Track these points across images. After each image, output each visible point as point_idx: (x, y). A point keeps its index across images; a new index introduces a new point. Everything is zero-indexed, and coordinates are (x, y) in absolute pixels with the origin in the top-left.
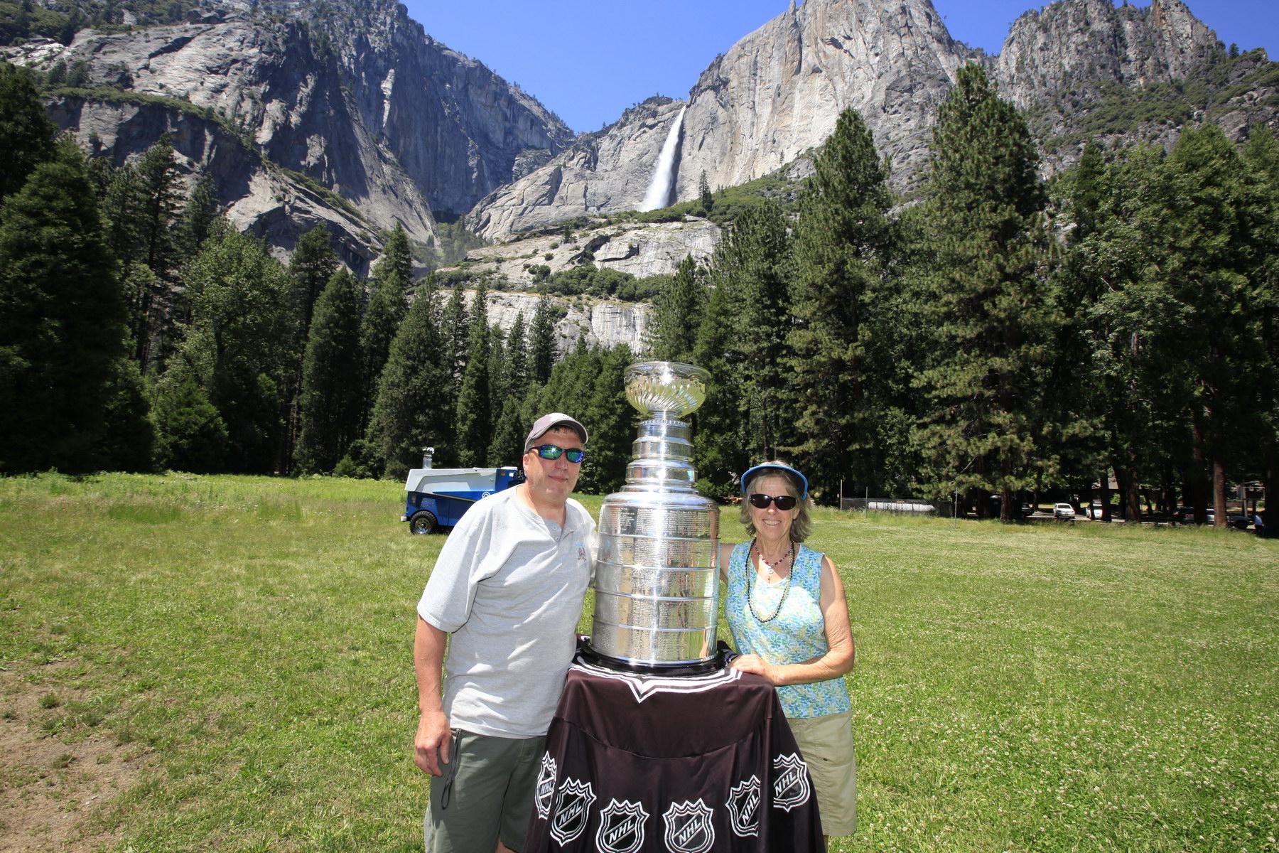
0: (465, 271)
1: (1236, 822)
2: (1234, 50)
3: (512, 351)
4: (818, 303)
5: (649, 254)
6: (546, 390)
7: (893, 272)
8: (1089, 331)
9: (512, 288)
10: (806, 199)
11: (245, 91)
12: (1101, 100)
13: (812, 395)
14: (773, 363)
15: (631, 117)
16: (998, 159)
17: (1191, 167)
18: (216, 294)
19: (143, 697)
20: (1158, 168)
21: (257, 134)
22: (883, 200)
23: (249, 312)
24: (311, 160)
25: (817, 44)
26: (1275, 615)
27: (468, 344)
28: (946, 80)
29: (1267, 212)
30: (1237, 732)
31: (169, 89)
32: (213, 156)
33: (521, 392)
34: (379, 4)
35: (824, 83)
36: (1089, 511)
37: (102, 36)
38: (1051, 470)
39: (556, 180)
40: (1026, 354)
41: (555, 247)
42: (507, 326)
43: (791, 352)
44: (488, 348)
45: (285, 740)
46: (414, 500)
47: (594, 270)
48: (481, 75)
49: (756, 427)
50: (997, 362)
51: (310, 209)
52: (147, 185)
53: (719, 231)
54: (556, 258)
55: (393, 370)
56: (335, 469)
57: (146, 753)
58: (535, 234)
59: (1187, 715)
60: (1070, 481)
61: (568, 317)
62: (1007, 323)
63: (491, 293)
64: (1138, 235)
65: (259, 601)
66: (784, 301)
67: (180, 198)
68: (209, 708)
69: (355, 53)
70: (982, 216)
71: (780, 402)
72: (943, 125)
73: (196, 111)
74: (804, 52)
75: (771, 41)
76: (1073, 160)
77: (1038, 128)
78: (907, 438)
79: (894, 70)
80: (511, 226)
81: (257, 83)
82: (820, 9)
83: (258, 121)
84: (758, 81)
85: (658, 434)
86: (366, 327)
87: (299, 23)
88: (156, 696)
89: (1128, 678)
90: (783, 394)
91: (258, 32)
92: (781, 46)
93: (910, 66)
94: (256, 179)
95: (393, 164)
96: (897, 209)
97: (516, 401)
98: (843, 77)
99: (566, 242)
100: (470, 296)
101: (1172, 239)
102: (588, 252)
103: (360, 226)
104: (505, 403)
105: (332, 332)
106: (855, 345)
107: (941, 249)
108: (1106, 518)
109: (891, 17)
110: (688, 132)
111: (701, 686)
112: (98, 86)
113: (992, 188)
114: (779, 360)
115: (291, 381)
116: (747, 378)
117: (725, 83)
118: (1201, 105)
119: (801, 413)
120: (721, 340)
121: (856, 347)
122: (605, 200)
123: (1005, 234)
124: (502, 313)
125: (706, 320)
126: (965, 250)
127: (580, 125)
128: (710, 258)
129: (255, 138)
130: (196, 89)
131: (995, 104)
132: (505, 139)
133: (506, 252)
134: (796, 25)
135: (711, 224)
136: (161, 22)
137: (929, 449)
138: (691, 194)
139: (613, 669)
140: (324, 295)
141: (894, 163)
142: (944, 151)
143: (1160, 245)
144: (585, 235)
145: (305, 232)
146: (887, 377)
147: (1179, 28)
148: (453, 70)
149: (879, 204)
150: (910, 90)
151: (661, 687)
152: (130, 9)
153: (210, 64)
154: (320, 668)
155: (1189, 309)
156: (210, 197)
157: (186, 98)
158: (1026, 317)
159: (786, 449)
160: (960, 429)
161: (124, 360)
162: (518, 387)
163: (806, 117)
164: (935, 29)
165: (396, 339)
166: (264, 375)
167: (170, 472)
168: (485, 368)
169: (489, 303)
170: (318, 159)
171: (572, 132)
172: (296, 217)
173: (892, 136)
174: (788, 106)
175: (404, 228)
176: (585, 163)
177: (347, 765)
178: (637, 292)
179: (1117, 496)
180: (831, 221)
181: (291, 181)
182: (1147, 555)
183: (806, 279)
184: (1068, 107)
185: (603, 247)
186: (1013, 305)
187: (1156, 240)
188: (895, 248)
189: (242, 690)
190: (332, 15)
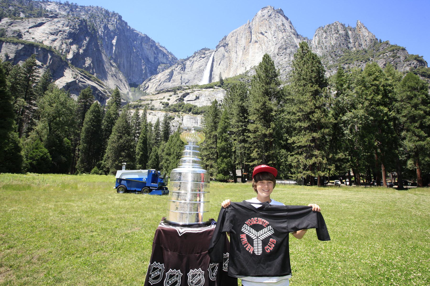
0: (140, 104)
1: (382, 276)
2: (381, 41)
4: (257, 115)
5: (202, 99)
6: (167, 144)
7: (281, 105)
8: (343, 125)
10: (253, 82)
11: (64, 41)
12: (343, 54)
13: (256, 145)
14: (243, 135)
15: (197, 54)
16: (312, 71)
17: (370, 75)
18: (49, 110)
19: (9, 251)
20: (360, 75)
21: (67, 56)
22: (278, 83)
24: (87, 65)
25: (256, 34)
26: (399, 213)
27: (140, 128)
28: (296, 46)
29: (392, 89)
30: (385, 249)
31: (36, 39)
32: (51, 62)
33: (158, 145)
34: (112, 15)
35: (259, 46)
36: (345, 183)
37: (12, 20)
38: (332, 169)
39: (171, 74)
40: (323, 132)
41: (171, 96)
42: (154, 122)
43: (249, 131)
45: (62, 264)
46: (119, 181)
47: (184, 104)
48: (147, 39)
49: (238, 156)
50: (315, 135)
51: (86, 81)
52: (26, 72)
53: (226, 92)
55: (113, 137)
56: (91, 172)
57: (8, 271)
58: (164, 92)
59: (370, 244)
60: (339, 173)
61: (175, 119)
62: (317, 122)
64: (355, 95)
65: (58, 216)
66: (247, 115)
67: (38, 77)
68: (35, 254)
69: (103, 30)
70: (308, 88)
71: (246, 148)
73: (45, 47)
75: (242, 32)
78: (287, 160)
79: (281, 43)
80: (156, 89)
81: (68, 39)
82: (257, 23)
83: (68, 51)
84: (238, 45)
85: (190, 149)
86: (104, 122)
87: (84, 19)
88: (14, 250)
89: (353, 233)
90: (247, 145)
91: (69, 22)
92: (245, 34)
93: (285, 41)
94: (66, 71)
95: (116, 67)
96: (282, 86)
97: (157, 148)
98: (265, 44)
99: (175, 94)
100: (141, 112)
101: (365, 97)
103: (103, 88)
104: (153, 148)
105: (92, 124)
106: (270, 129)
107: (296, 99)
108: (350, 185)
110: (215, 60)
111: (201, 230)
112: (9, 37)
113: (311, 80)
114: (245, 134)
115: (76, 140)
116: (235, 140)
117: (227, 45)
118: (372, 57)
119: (253, 151)
120: (226, 127)
121: (270, 130)
122: (188, 81)
123: (316, 94)
124: (152, 118)
125: (221, 121)
126: (303, 99)
127: (180, 56)
128: (222, 100)
130: (46, 40)
132: (154, 60)
133: (154, 97)
134: (250, 27)
135: (223, 89)
136: (34, 17)
137: (294, 163)
138: (216, 80)
139: (173, 226)
140: (89, 111)
141: (281, 71)
142: (296, 68)
143: (362, 98)
144: (181, 92)
145: (83, 89)
146: (280, 140)
147: (364, 34)
148: (137, 37)
149: (276, 84)
150: (286, 49)
151: (187, 231)
152: (23, 12)
153: (51, 32)
154: (79, 238)
155: (372, 118)
157: (42, 42)
158: (323, 120)
159: (248, 163)
161: (13, 132)
162: (157, 143)
164: (293, 31)
166: (66, 138)
167: (29, 173)
168: (146, 137)
169: (148, 115)
170: (89, 65)
171: (177, 59)
172: (80, 84)
173: (280, 63)
175: (118, 88)
176: (181, 69)
177: (85, 271)
178: (198, 111)
179: (354, 177)
180: (261, 89)
181: (79, 72)
182: (362, 196)
183: (254, 108)
184: (334, 56)
185: (187, 96)
186: (319, 116)
187: (361, 97)
188: (282, 98)
189: (48, 247)
190: (96, 17)
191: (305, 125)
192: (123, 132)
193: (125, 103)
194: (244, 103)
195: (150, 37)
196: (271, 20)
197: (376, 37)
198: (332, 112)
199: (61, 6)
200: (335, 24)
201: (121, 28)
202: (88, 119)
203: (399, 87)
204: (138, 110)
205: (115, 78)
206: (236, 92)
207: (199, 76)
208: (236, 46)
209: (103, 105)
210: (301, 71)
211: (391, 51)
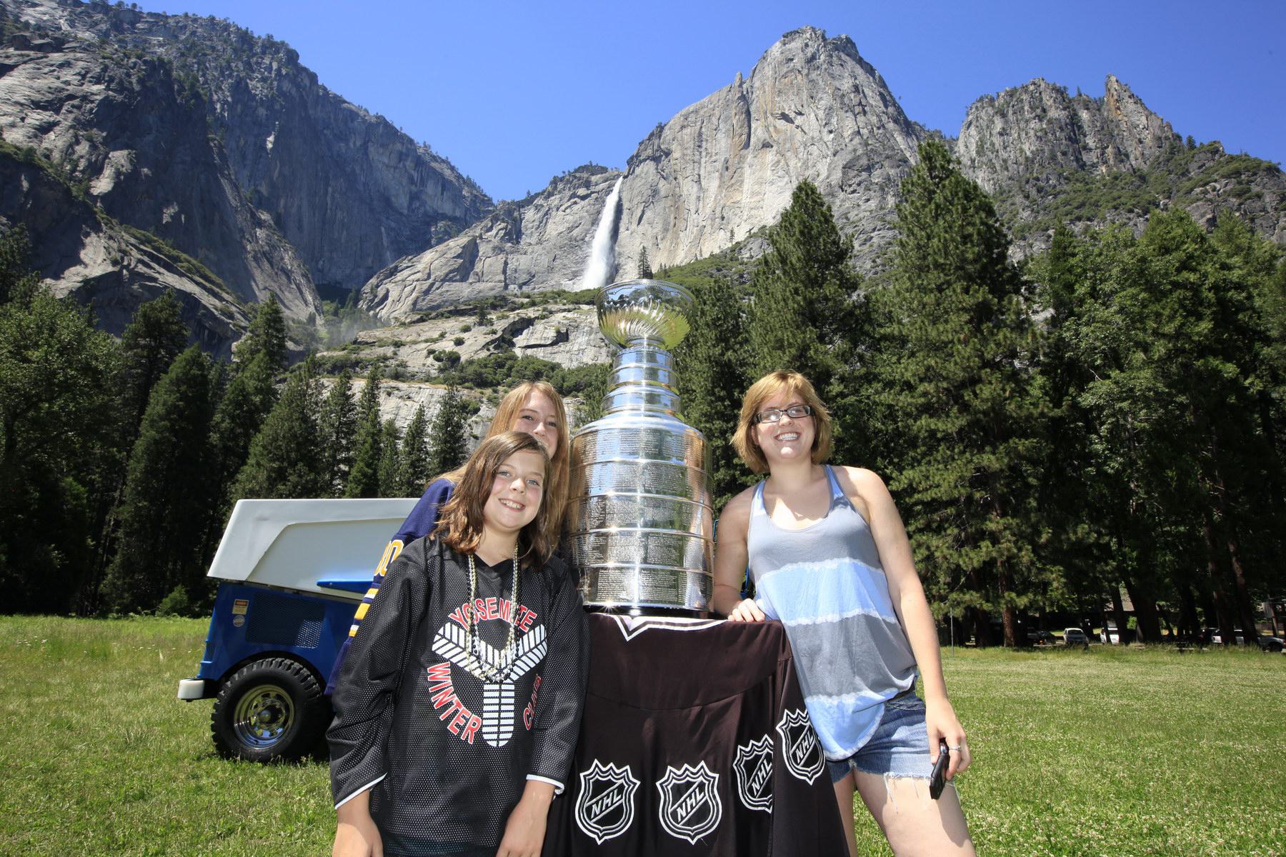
0: (353, 356)
3: (410, 453)
5: (579, 340)
7: (861, 358)
9: (412, 377)
12: (1065, 187)
16: (966, 238)
17: (1165, 250)
20: (1130, 250)
21: (93, 183)
23: (59, 396)
24: (166, 219)
25: (766, 118)
27: (354, 443)
28: (905, 161)
29: (1247, 298)
36: (1103, 637)
38: (1055, 584)
39: (470, 255)
41: (466, 329)
42: (404, 424)
44: (380, 449)
47: (514, 358)
48: (385, 132)
51: (157, 275)
54: (467, 343)
56: (160, 606)
60: (1079, 602)
61: (480, 413)
63: (386, 383)
69: (230, 99)
70: (954, 298)
72: (907, 201)
74: (753, 125)
75: (717, 112)
76: (1043, 246)
77: (1004, 213)
79: (850, 148)
80: (415, 304)
82: (769, 83)
83: (95, 169)
87: (160, 60)
93: (867, 145)
95: (270, 227)
99: (481, 324)
100: (358, 386)
101: (1155, 325)
102: (507, 336)
103: (221, 299)
105: (173, 425)
109: (843, 95)
110: (626, 205)
113: (962, 268)
117: (668, 154)
124: (398, 408)
126: (939, 334)
127: (500, 191)
129: (90, 187)
130: (13, 125)
131: (958, 183)
133: (406, 335)
134: (743, 98)
140: (165, 379)
141: (856, 244)
142: (909, 229)
143: (1145, 330)
144: (504, 317)
145: (148, 300)
147: (1134, 119)
150: (869, 169)
153: (37, 97)
156: (20, 254)
158: (1011, 407)
160: (950, 539)
163: (758, 194)
164: (891, 110)
165: (260, 436)
166: (70, 479)
168: (375, 471)
169: (382, 398)
170: (171, 217)
171: (490, 200)
173: (852, 216)
174: (737, 181)
178: (565, 385)
180: (790, 302)
181: (133, 241)
184: (1033, 192)
185: (525, 332)
190: (205, 55)
191: (951, 424)
192: (288, 457)
193: (300, 352)
194: (730, 353)
195: (398, 129)
196: (814, 75)
197: (1175, 131)
198: (1040, 380)
199: (79, 10)
200: (1032, 88)
201: (294, 91)
202: (160, 409)
203: (1271, 292)
204: (350, 378)
205: (266, 265)
206: (703, 313)
207: (566, 262)
208: (696, 158)
209: (220, 360)
210: (929, 238)
211: (1228, 176)
